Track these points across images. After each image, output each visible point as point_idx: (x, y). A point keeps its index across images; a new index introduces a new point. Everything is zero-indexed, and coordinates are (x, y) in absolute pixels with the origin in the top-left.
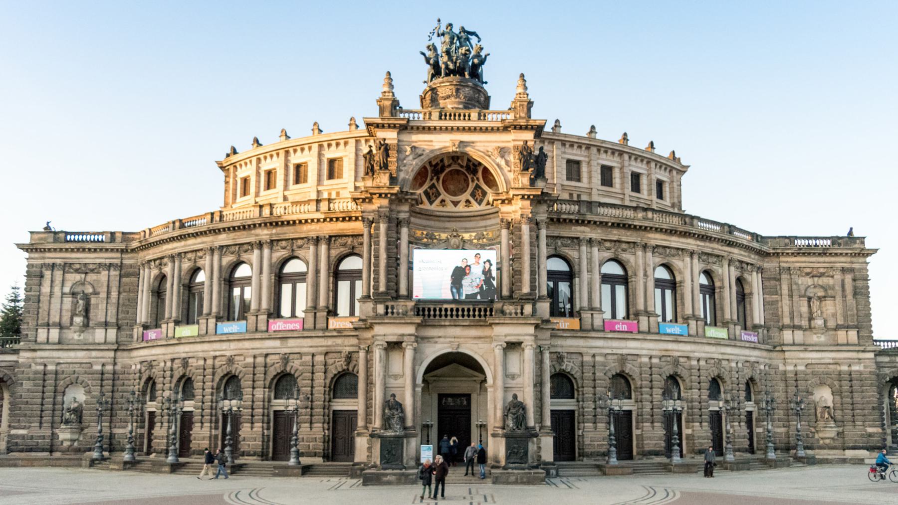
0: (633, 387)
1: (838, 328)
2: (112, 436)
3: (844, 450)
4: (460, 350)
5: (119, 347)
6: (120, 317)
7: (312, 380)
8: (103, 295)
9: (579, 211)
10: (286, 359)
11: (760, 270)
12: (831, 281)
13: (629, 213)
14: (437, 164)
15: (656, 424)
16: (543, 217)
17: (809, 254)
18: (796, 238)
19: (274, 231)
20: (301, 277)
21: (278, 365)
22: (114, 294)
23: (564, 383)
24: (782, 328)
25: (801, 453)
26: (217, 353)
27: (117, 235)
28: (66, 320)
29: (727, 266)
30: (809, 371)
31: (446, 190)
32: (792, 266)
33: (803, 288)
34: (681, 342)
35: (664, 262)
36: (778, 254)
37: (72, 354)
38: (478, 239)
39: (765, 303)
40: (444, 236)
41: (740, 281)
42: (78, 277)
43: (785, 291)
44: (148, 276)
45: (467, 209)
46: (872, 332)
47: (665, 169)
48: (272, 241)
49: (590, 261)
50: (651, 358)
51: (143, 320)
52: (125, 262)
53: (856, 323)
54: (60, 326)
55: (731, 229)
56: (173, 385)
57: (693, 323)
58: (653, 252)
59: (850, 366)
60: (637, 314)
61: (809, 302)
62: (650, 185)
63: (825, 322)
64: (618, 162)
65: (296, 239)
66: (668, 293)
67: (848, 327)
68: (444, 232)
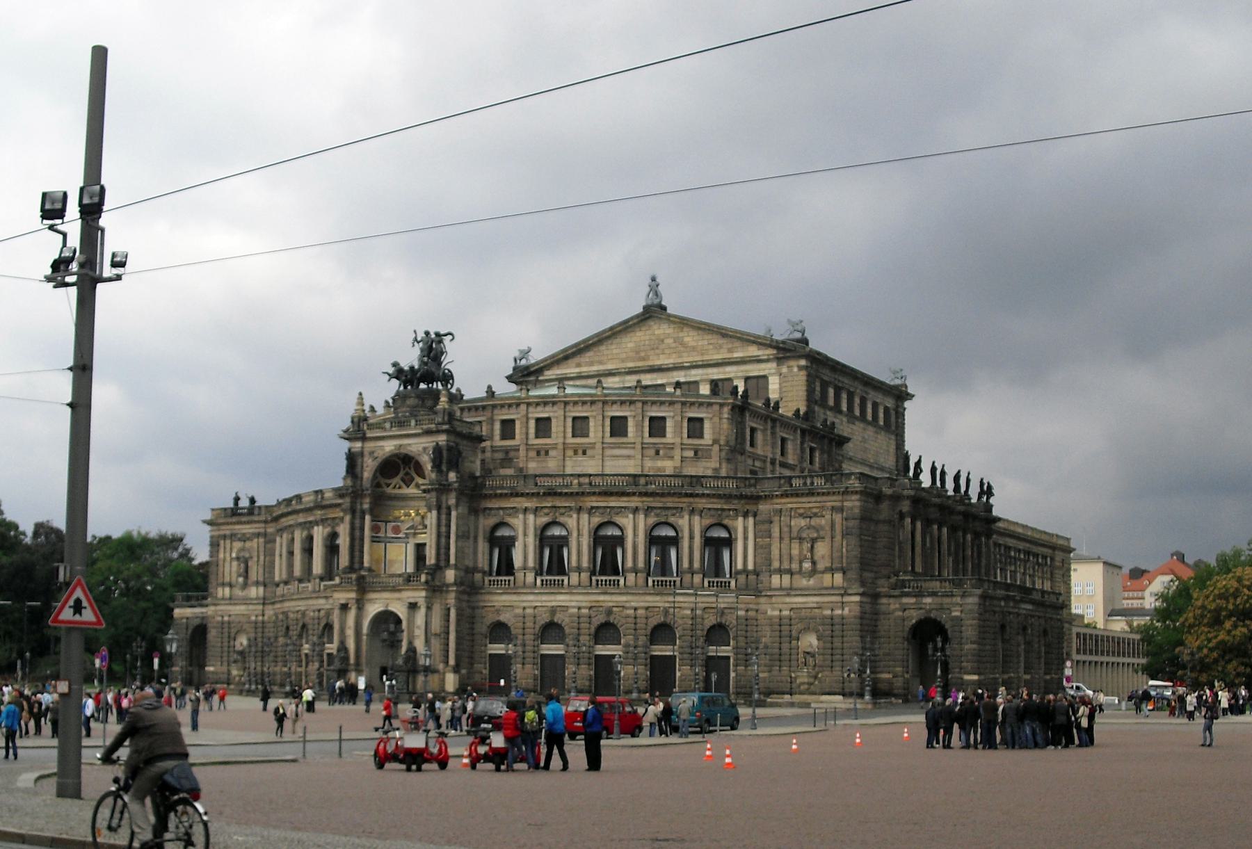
5: (264, 601)
12: (823, 522)
16: (452, 501)
17: (797, 495)
22: (262, 558)
23: (500, 631)
24: (771, 573)
29: (687, 517)
32: (784, 507)
33: (795, 530)
37: (238, 607)
48: (322, 520)
54: (231, 585)
57: (631, 577)
58: (590, 514)
63: (814, 563)
67: (832, 570)
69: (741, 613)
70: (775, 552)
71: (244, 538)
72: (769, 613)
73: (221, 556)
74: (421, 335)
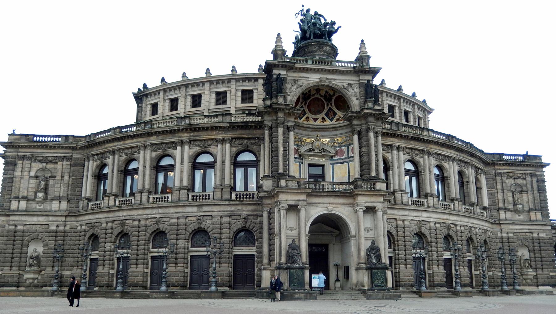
0: (425, 242)
1: (529, 211)
2: (62, 276)
3: (538, 286)
4: (333, 212)
5: (68, 215)
6: (69, 193)
7: (221, 234)
8: (58, 178)
9: (391, 128)
10: (200, 220)
11: (485, 173)
12: (524, 182)
13: (418, 132)
14: (306, 93)
15: (440, 266)
18: (503, 154)
19: (192, 134)
20: (211, 165)
21: (195, 224)
22: (66, 178)
24: (499, 210)
25: (518, 288)
26: (149, 216)
27: (70, 137)
28: (31, 195)
30: (515, 237)
31: (310, 111)
32: (503, 172)
33: (509, 185)
34: (451, 214)
35: (438, 163)
36: (494, 163)
37: (35, 218)
38: (331, 143)
39: (490, 194)
40: (308, 140)
41: (477, 179)
42: (40, 166)
43: (499, 187)
44: (91, 166)
45: (322, 123)
46: (549, 213)
47: (421, 110)
48: (190, 141)
49: (399, 159)
50: (435, 224)
51: (88, 195)
52: (74, 155)
53: (540, 208)
54: (26, 199)
55: (471, 145)
56: (113, 240)
57: (456, 202)
59: (538, 234)
60: (426, 196)
61: (513, 194)
62: (414, 118)
63: (523, 205)
64: (397, 103)
65: (207, 140)
66: (440, 182)
67: (536, 210)
68: (309, 138)
69: (490, 233)
70: (500, 198)
71: (46, 160)
72: (499, 234)
73: (18, 173)
74: (305, 11)
